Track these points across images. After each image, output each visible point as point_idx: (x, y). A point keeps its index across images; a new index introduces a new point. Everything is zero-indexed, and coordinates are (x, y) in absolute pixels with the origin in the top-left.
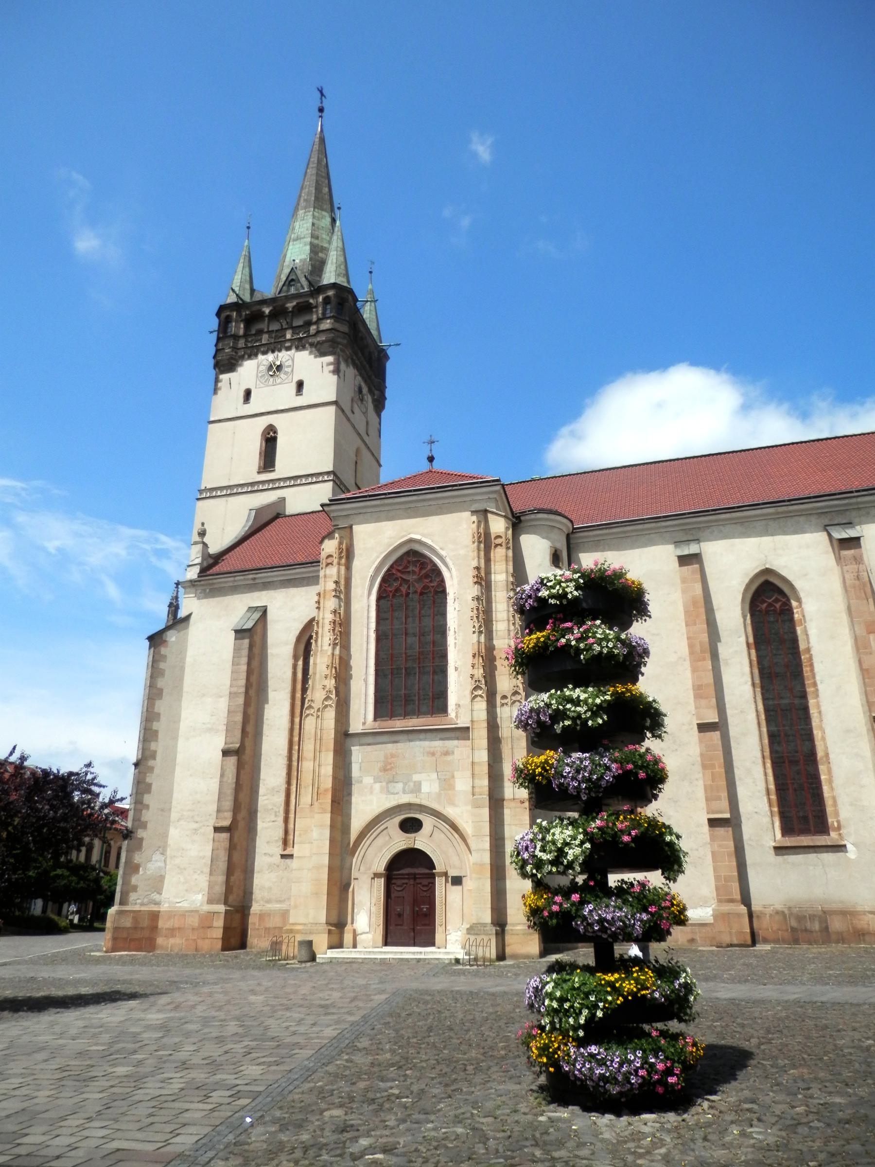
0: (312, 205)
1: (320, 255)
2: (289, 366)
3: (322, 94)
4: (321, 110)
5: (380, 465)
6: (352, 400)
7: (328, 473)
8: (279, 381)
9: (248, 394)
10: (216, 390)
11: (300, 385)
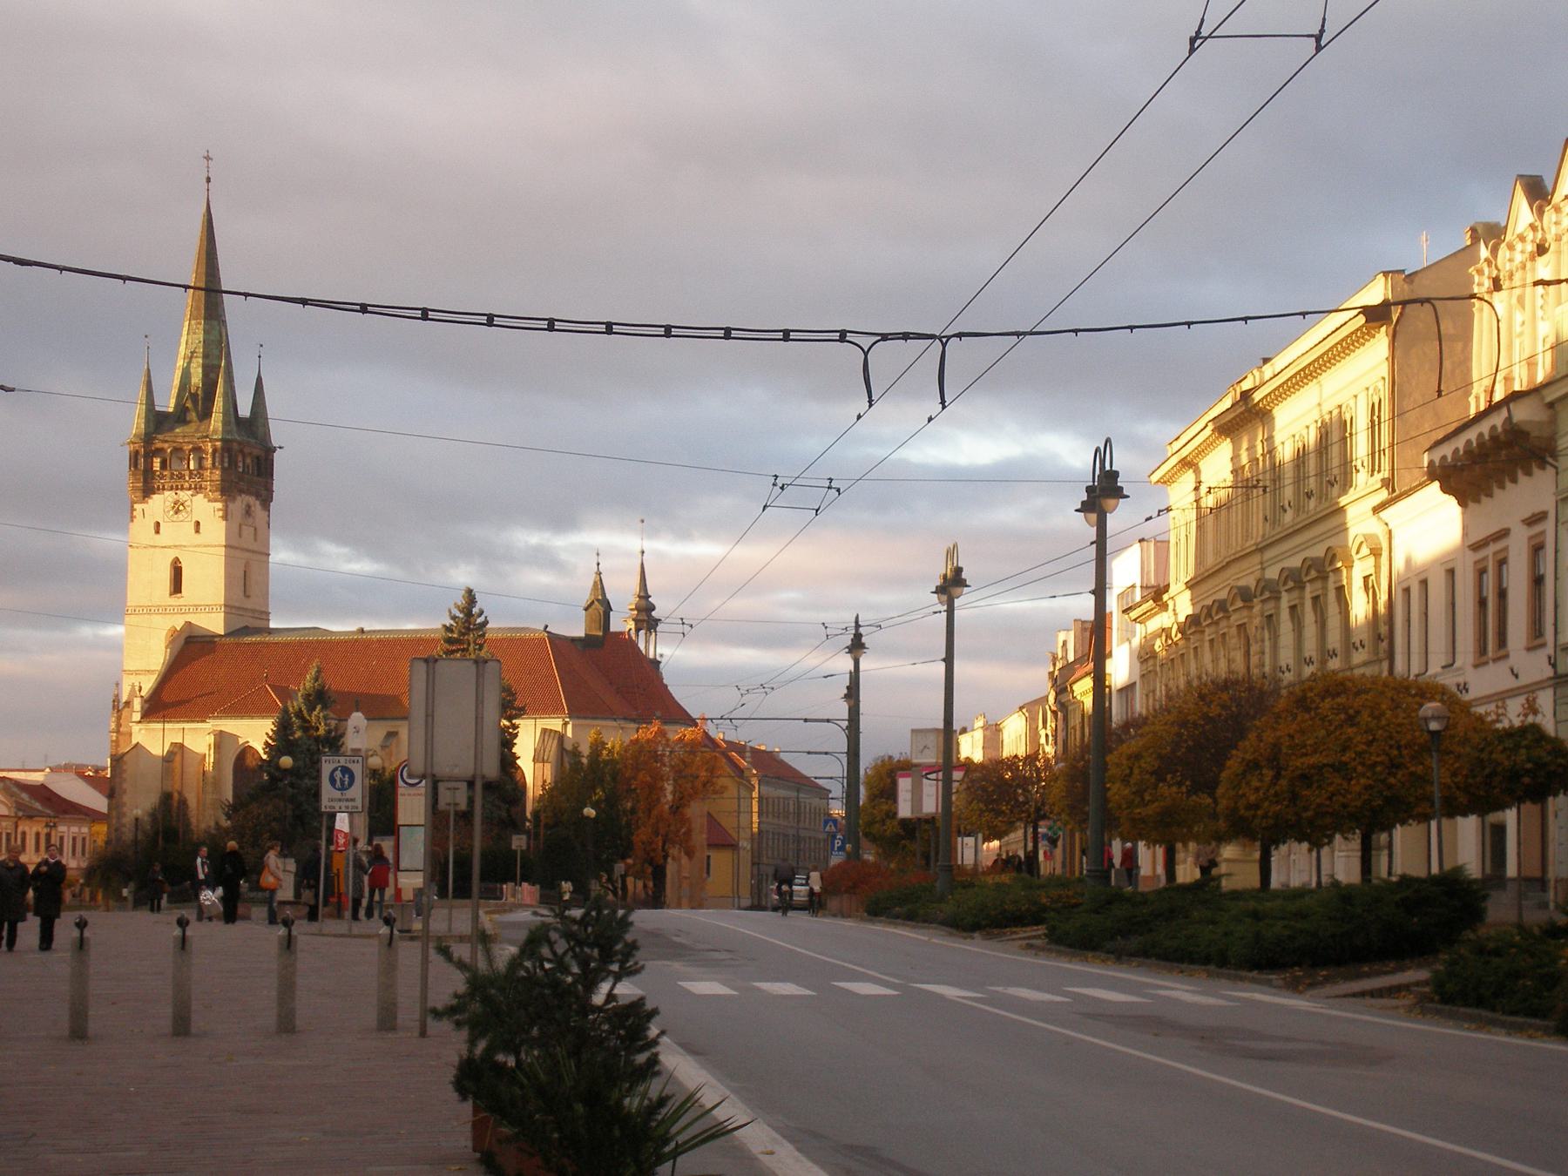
0: (203, 315)
1: (212, 375)
2: (189, 506)
3: (208, 158)
4: (208, 180)
5: (269, 555)
6: (240, 525)
7: (220, 606)
8: (180, 516)
9: (158, 524)
10: (132, 518)
11: (198, 524)
